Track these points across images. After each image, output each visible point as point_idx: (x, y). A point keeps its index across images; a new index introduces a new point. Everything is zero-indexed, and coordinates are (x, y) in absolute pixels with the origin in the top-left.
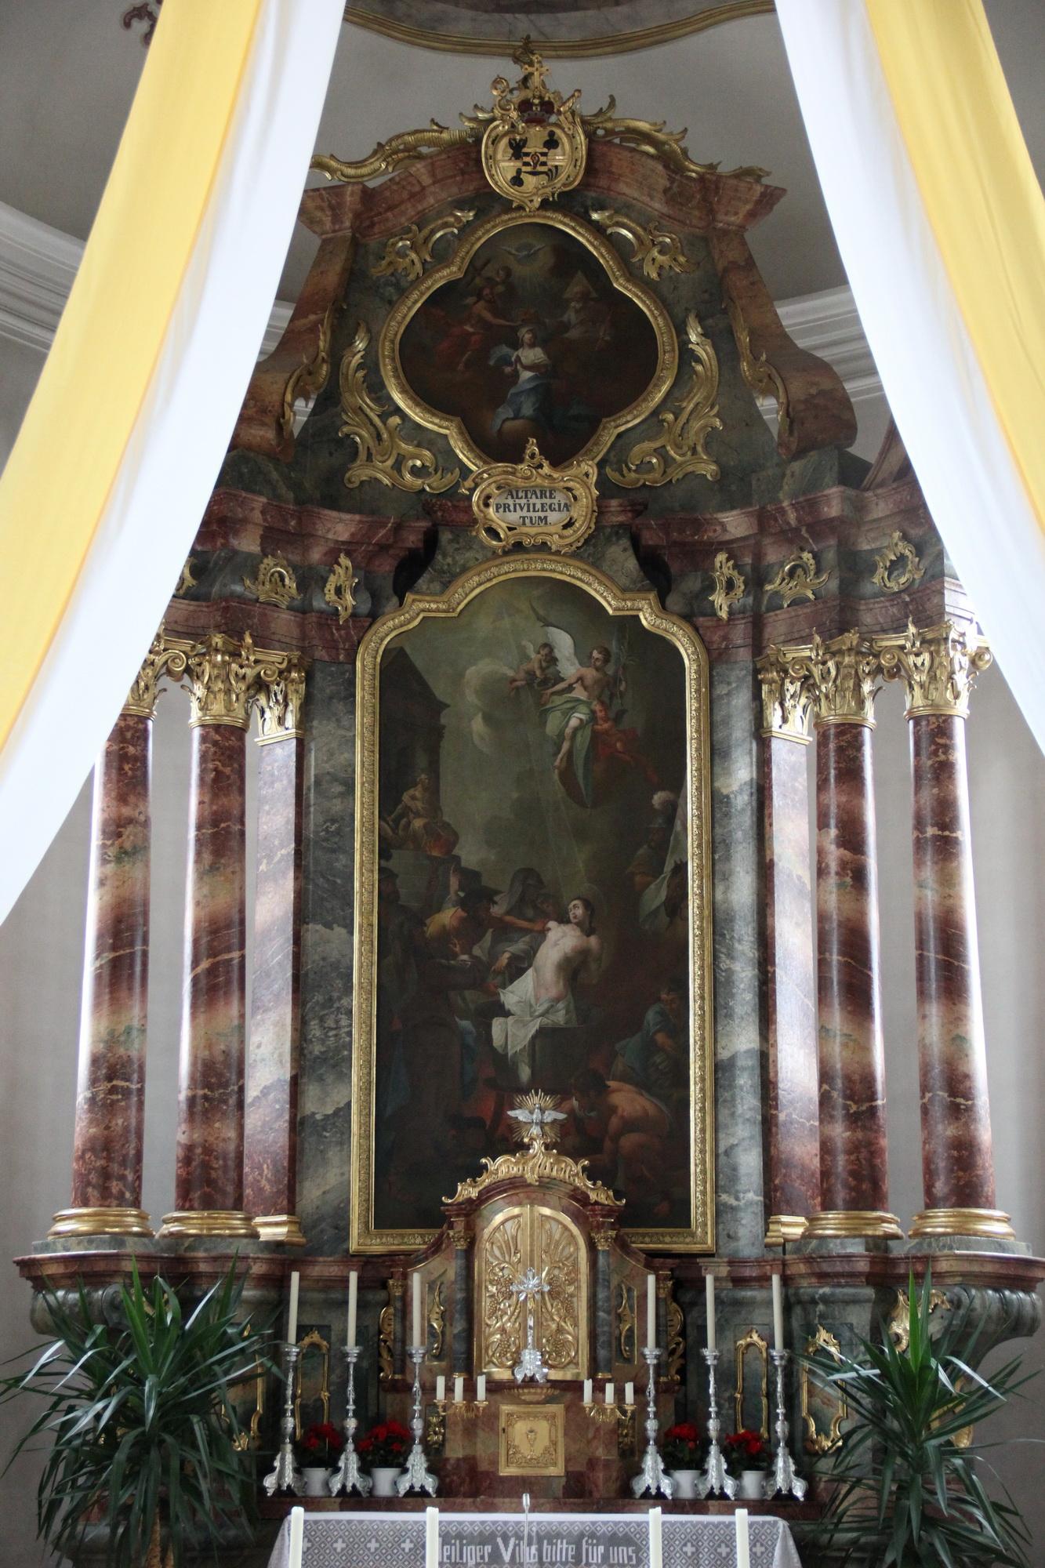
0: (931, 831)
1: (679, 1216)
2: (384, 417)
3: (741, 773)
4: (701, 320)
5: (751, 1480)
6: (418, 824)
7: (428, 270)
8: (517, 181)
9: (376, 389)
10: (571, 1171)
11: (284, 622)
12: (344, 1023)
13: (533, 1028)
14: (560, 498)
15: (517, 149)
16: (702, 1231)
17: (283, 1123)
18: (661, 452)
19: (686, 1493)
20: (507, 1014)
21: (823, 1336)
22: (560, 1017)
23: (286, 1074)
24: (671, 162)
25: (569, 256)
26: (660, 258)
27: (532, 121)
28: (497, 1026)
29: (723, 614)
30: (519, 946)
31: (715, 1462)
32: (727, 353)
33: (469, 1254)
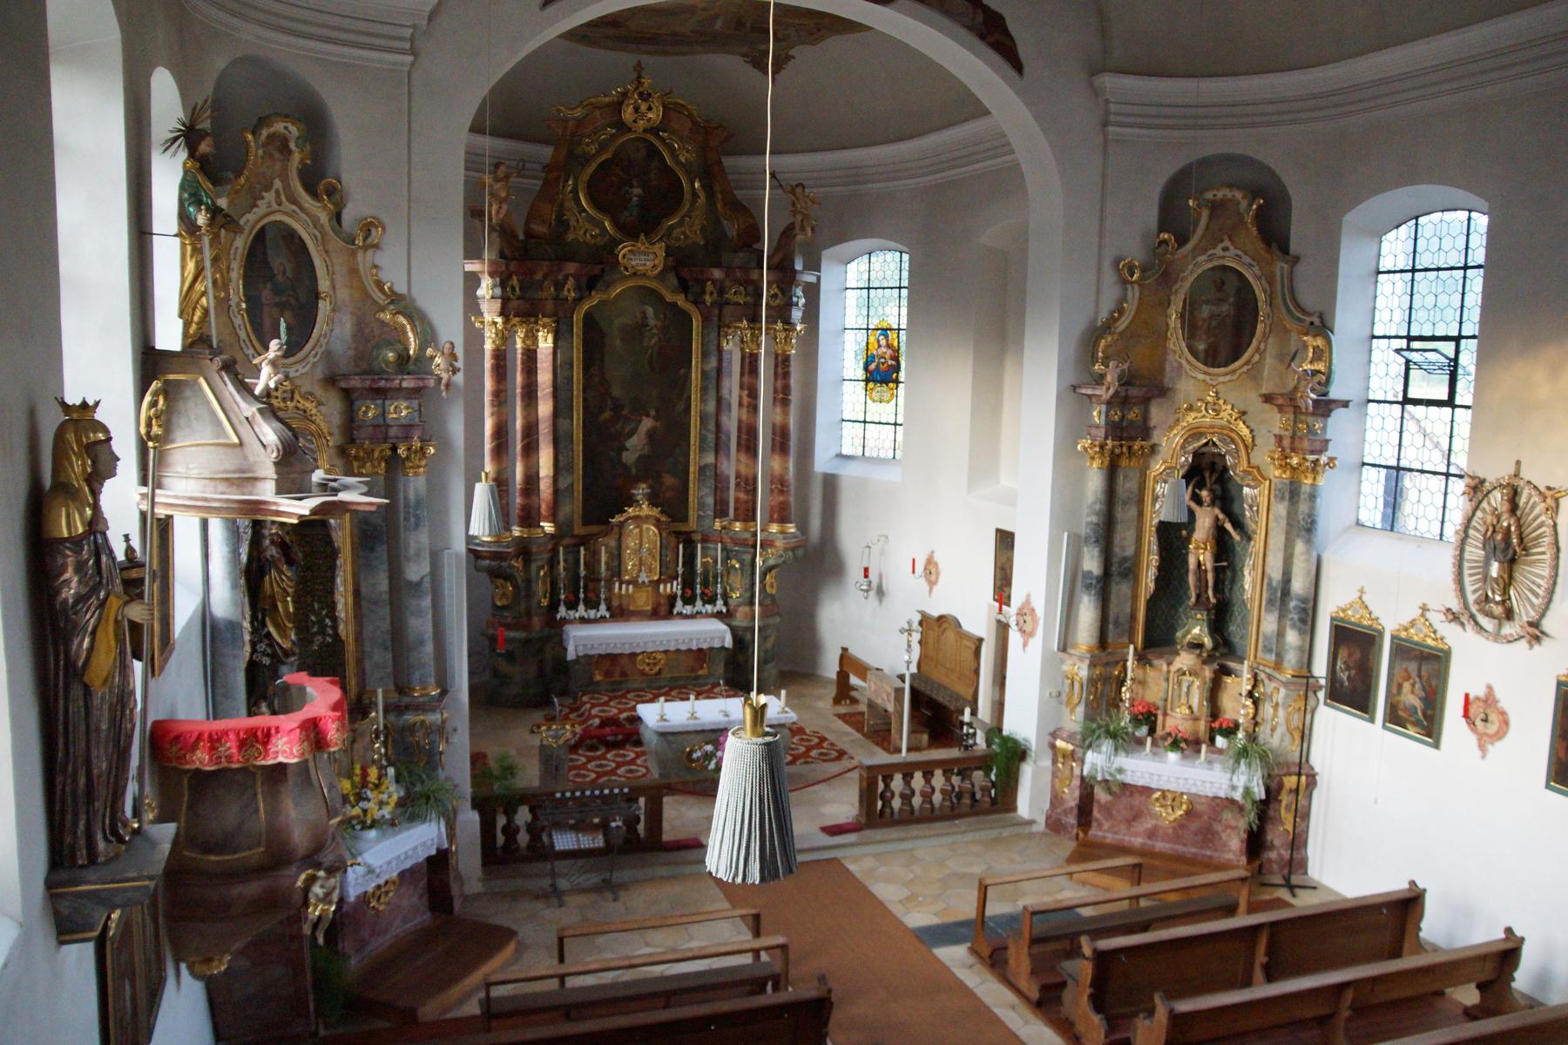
0: (781, 396)
1: (685, 519)
2: (580, 213)
3: (713, 363)
4: (700, 181)
5: (709, 608)
6: (596, 379)
7: (599, 152)
8: (635, 121)
9: (577, 200)
10: (655, 512)
11: (550, 306)
12: (570, 453)
13: (637, 454)
14: (651, 256)
15: (637, 109)
16: (692, 524)
17: (550, 491)
18: (684, 233)
19: (689, 613)
20: (627, 450)
21: (734, 562)
22: (646, 451)
23: (551, 473)
24: (690, 116)
25: (653, 153)
26: (688, 155)
27: (643, 100)
28: (624, 454)
29: (708, 304)
30: (633, 425)
31: (699, 603)
32: (710, 195)
33: (619, 540)
